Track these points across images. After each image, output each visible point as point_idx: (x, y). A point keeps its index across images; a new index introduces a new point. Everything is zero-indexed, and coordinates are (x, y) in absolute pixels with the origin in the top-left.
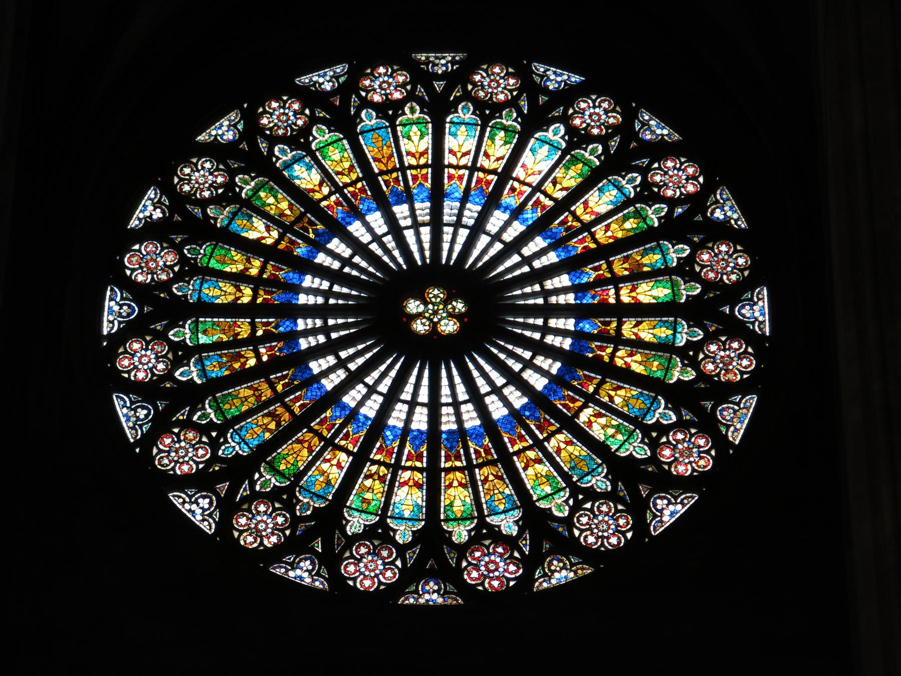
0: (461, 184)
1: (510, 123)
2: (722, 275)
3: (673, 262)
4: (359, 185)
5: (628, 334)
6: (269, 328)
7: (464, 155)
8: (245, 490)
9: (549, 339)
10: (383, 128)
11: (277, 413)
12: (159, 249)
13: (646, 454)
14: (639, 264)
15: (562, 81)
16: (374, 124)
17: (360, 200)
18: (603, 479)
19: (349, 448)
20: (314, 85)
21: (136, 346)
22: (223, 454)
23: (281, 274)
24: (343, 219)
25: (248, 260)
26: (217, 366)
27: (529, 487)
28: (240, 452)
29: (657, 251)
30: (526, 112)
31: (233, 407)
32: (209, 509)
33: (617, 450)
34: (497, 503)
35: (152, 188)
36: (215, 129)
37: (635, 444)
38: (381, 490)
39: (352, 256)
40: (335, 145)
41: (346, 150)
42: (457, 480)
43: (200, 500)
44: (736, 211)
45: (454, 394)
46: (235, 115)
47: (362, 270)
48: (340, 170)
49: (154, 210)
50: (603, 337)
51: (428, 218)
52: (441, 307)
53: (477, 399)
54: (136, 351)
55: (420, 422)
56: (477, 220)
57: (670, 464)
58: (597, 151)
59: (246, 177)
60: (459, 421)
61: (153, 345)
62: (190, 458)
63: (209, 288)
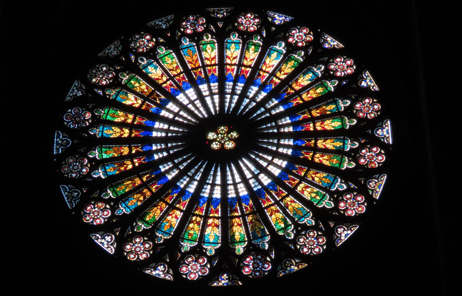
0: (233, 73)
1: (257, 41)
2: (367, 114)
3: (342, 109)
4: (181, 75)
5: (320, 145)
6: (138, 149)
7: (234, 58)
9: (280, 150)
10: (192, 46)
11: (144, 192)
12: (81, 111)
13: (331, 206)
14: (325, 110)
15: (282, 20)
16: (188, 45)
17: (182, 83)
18: (310, 219)
19: (181, 208)
21: (71, 161)
22: (117, 213)
24: (174, 93)
26: (113, 169)
27: (273, 224)
28: (126, 212)
30: (264, 36)
31: (121, 190)
32: (111, 241)
33: (317, 204)
34: (257, 233)
35: (76, 81)
36: (107, 50)
37: (326, 201)
38: (198, 229)
39: (179, 111)
40: (169, 56)
41: (174, 58)
42: (236, 222)
43: (106, 237)
44: (372, 82)
45: (234, 179)
46: (117, 42)
47: (185, 118)
48: (171, 68)
49: (78, 92)
50: (308, 148)
51: (217, 91)
52: (225, 135)
54: (71, 163)
55: (217, 194)
56: (242, 91)
57: (344, 210)
58: (301, 54)
60: (237, 192)
61: (79, 161)
62: (100, 216)
63: (107, 130)
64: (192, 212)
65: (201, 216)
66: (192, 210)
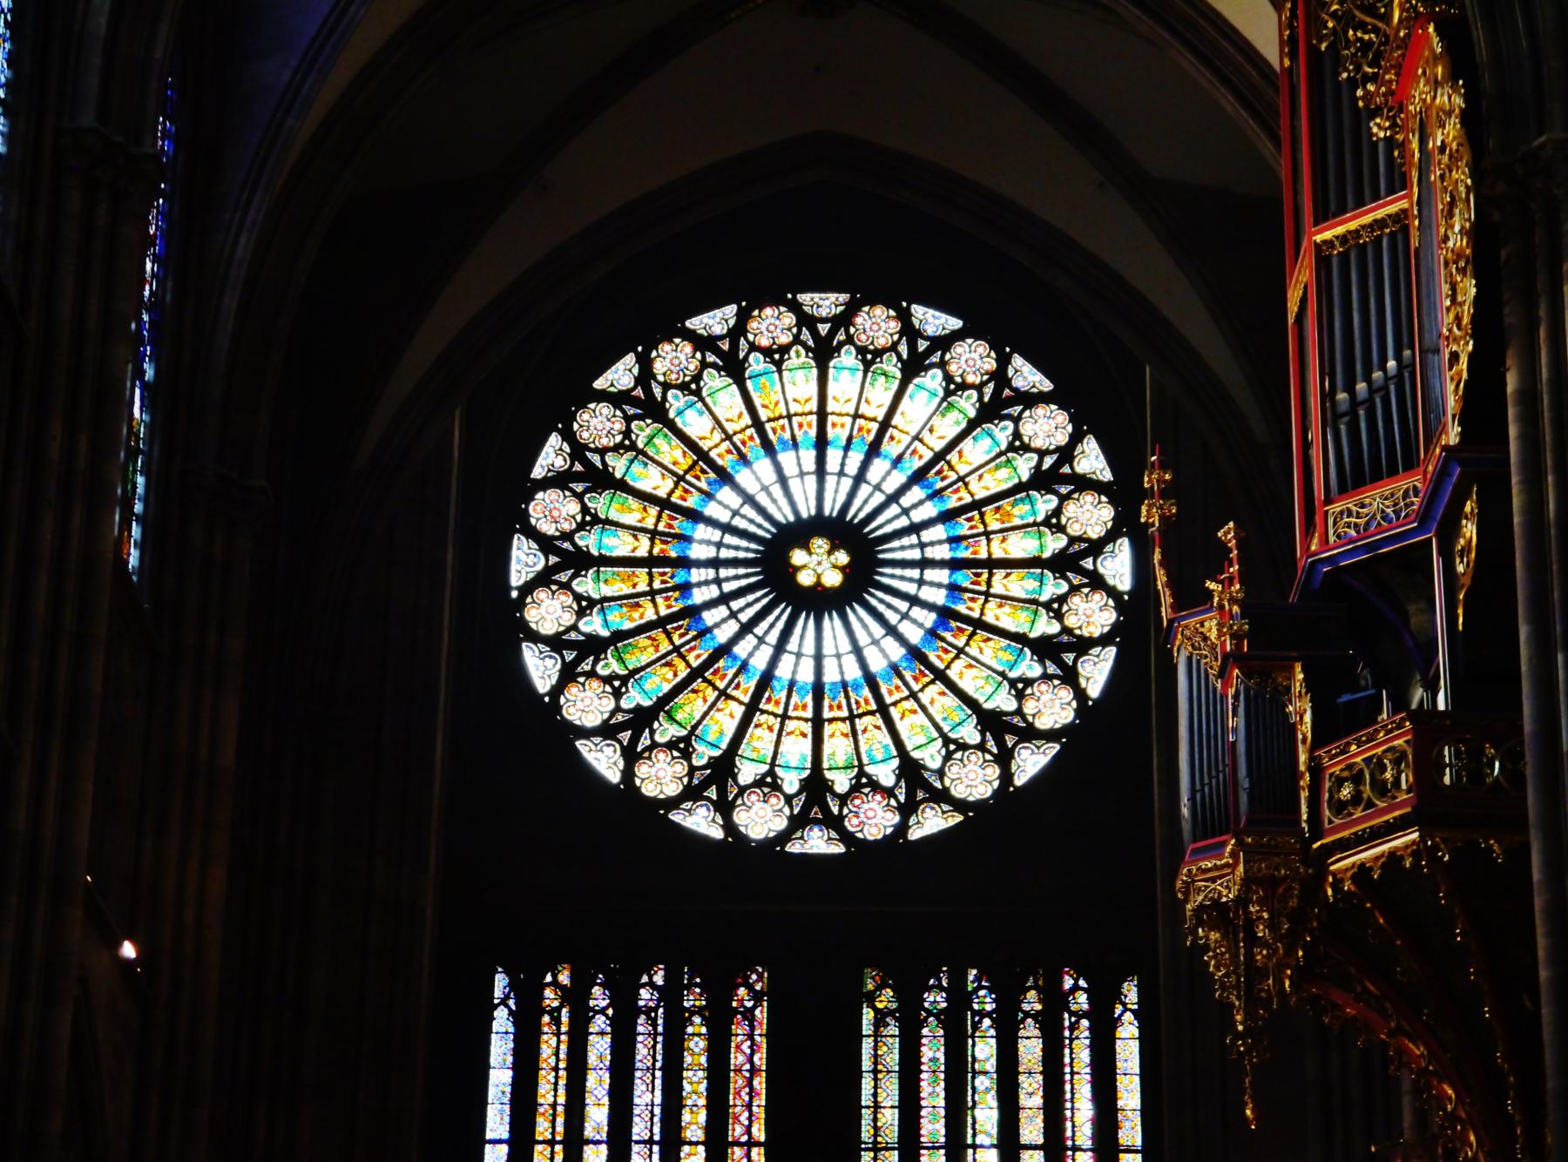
6: (665, 578)
8: (646, 739)
20: (705, 328)
23: (675, 523)
25: (645, 509)
29: (1027, 501)
52: (825, 557)
53: (857, 651)
55: (806, 675)
59: (642, 423)
64: (761, 706)
65: (776, 716)
66: (760, 702)
